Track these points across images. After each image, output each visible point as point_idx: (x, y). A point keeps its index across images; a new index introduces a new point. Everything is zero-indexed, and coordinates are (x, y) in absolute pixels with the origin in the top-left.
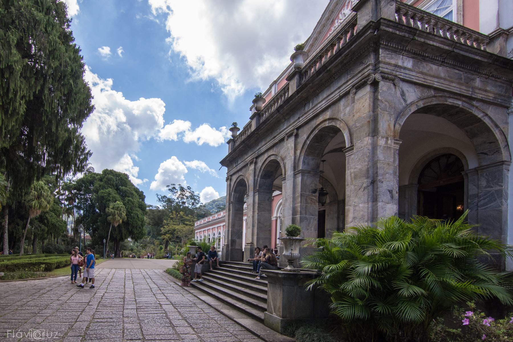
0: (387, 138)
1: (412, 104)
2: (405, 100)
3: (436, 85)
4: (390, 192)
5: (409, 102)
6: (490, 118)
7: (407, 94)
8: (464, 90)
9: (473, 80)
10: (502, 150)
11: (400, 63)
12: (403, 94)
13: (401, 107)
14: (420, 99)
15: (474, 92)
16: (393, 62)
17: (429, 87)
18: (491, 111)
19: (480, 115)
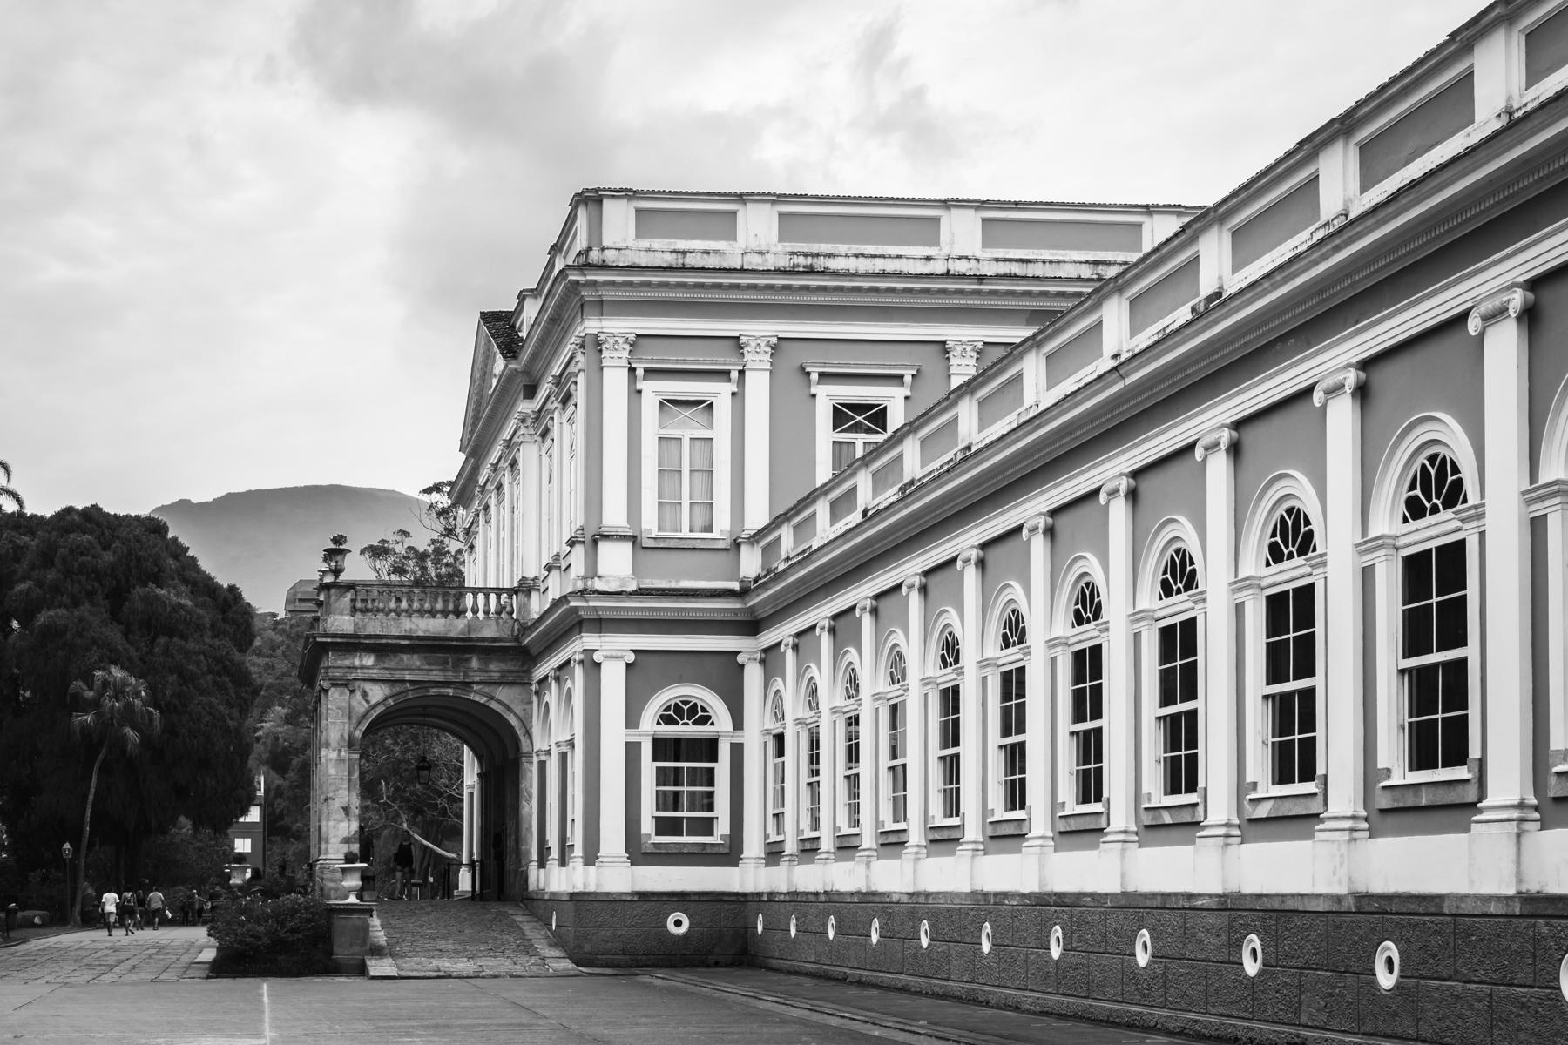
0: (340, 750)
1: (376, 705)
2: (368, 702)
3: (408, 677)
4: (345, 809)
5: (373, 702)
6: (499, 702)
7: (370, 694)
8: (451, 676)
9: (468, 660)
10: (522, 738)
11: (357, 662)
12: (365, 695)
13: (362, 710)
14: (386, 699)
15: (466, 675)
16: (347, 663)
17: (403, 681)
18: (503, 693)
19: (483, 700)
